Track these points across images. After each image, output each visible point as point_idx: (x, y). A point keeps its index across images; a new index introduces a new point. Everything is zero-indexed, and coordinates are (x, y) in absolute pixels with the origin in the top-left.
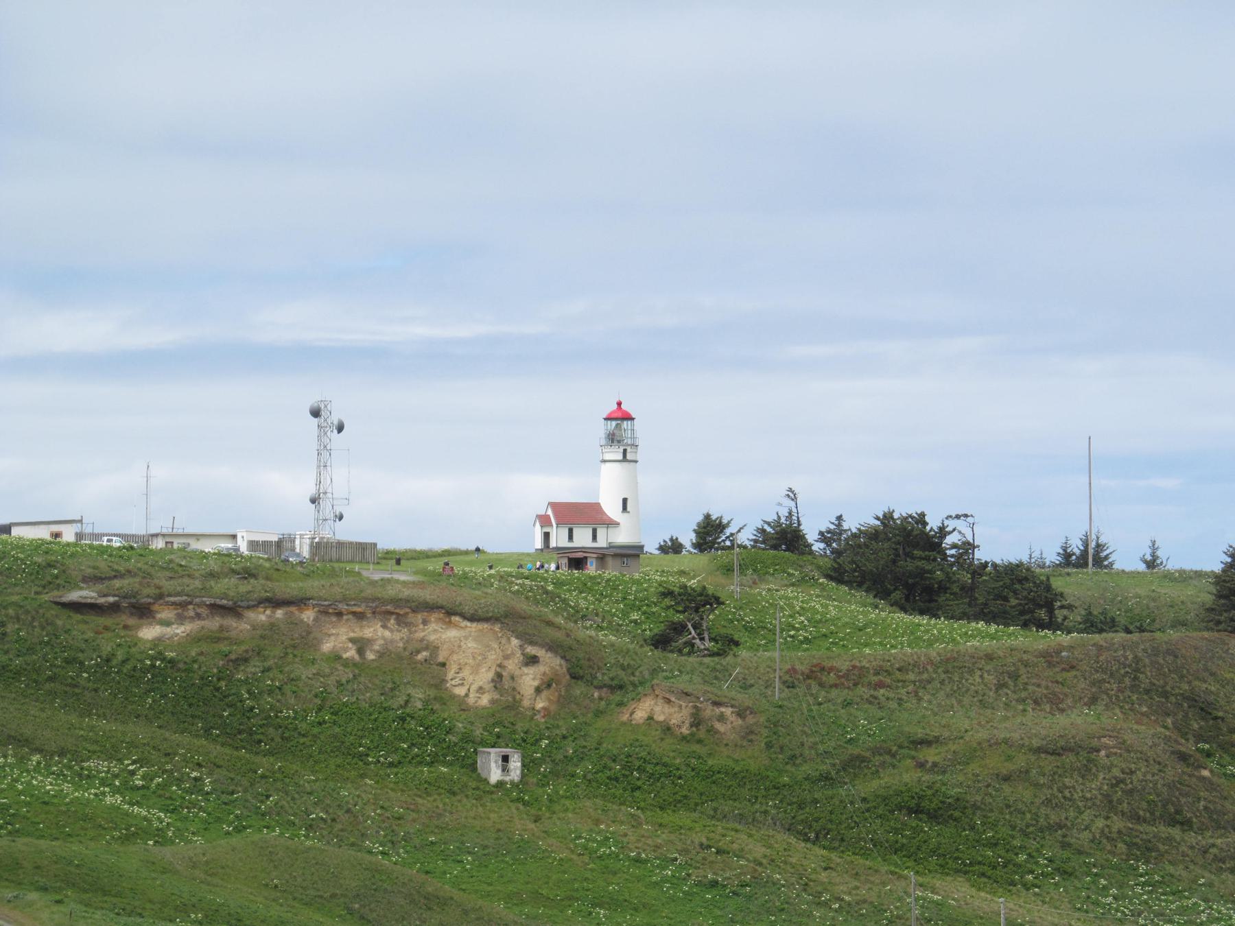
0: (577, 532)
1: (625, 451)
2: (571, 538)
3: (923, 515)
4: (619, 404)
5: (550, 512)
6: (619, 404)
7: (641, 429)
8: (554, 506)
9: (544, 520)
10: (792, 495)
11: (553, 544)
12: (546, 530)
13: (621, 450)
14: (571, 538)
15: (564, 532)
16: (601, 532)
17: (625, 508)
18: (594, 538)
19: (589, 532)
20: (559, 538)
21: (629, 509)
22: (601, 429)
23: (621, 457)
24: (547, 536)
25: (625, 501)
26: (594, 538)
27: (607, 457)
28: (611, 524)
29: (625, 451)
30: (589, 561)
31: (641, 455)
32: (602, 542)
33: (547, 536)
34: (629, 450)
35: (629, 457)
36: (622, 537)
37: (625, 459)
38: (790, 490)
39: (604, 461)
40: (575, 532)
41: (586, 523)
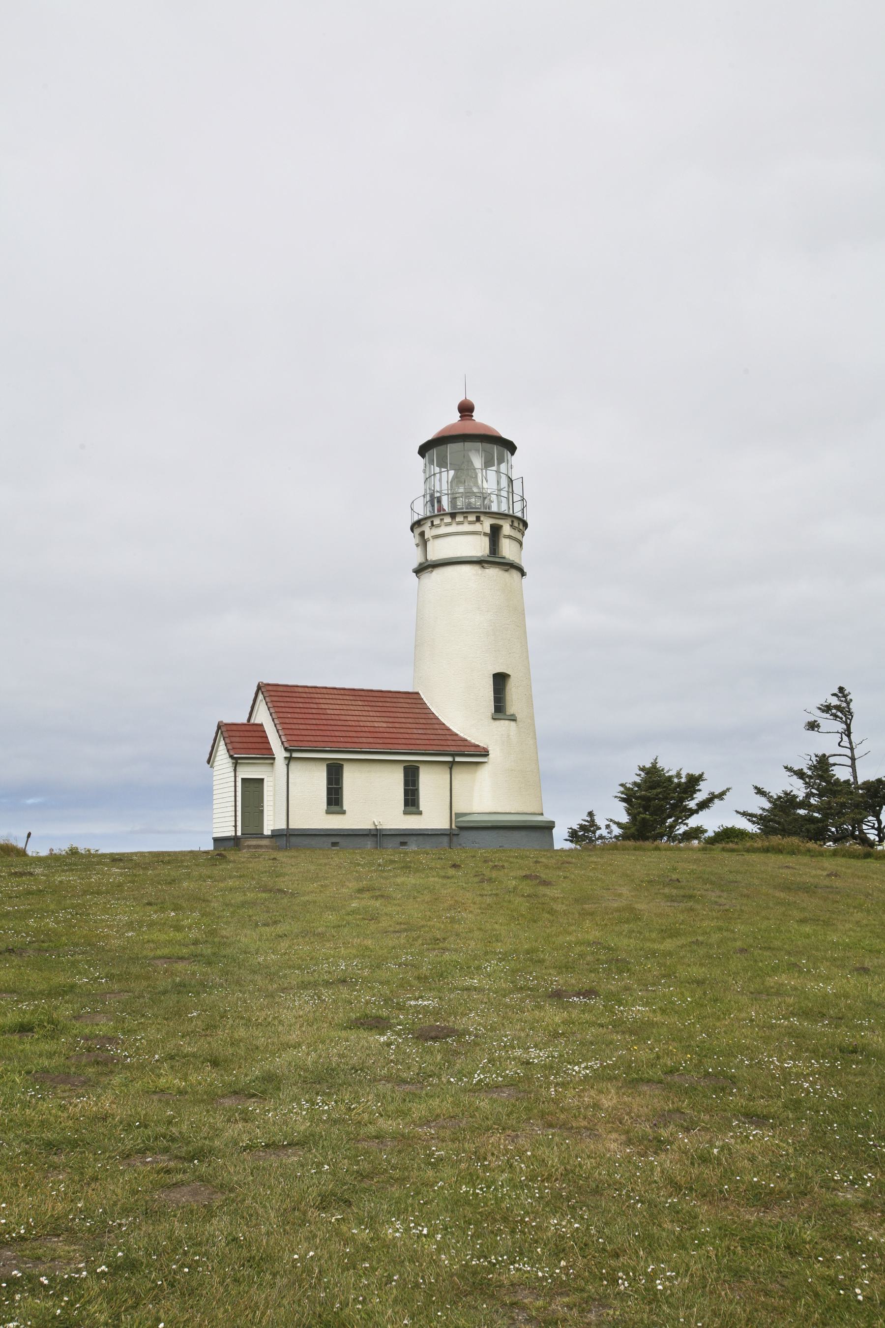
1: (495, 531)
2: (335, 799)
4: (466, 410)
6: (466, 410)
7: (534, 476)
9: (244, 742)
12: (249, 772)
13: (486, 525)
14: (335, 799)
17: (500, 708)
18: (411, 801)
19: (395, 779)
20: (296, 796)
21: (511, 709)
22: (412, 482)
23: (479, 547)
25: (500, 680)
26: (411, 801)
27: (439, 550)
28: (463, 755)
29: (495, 531)
31: (529, 550)
32: (433, 816)
33: (252, 791)
34: (507, 529)
35: (507, 549)
37: (493, 559)
38: (841, 689)
41: (375, 746)
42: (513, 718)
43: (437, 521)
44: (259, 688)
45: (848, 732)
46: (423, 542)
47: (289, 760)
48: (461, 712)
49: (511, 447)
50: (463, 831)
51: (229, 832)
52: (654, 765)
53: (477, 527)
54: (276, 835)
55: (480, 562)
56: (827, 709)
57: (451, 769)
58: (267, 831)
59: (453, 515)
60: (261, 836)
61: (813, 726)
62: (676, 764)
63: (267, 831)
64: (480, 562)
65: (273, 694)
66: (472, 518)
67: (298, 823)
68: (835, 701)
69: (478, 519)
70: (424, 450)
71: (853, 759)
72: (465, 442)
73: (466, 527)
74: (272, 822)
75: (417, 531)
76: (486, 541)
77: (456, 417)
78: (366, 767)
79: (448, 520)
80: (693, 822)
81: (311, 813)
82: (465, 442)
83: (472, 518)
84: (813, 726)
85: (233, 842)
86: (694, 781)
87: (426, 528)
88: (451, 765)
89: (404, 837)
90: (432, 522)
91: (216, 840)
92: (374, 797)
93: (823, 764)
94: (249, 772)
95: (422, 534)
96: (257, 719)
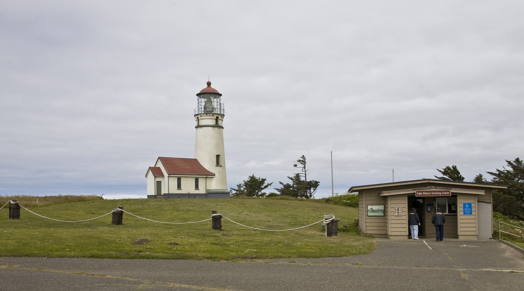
0: (183, 181)
1: (217, 118)
2: (179, 186)
3: (455, 168)
4: (209, 84)
5: (160, 165)
6: (209, 84)
8: (164, 160)
9: (156, 172)
10: (303, 161)
11: (164, 191)
12: (158, 179)
14: (179, 186)
15: (174, 182)
16: (201, 182)
17: (218, 164)
18: (197, 187)
19: (192, 182)
20: (169, 185)
21: (221, 164)
23: (213, 122)
24: (159, 185)
26: (197, 187)
27: (202, 123)
28: (208, 175)
29: (217, 118)
30: (461, 203)
31: (225, 122)
32: (202, 190)
34: (220, 118)
35: (220, 123)
36: (214, 185)
38: (303, 156)
39: (198, 126)
40: (183, 180)
42: (221, 166)
44: (159, 158)
45: (305, 168)
46: (198, 120)
47: (169, 177)
48: (208, 164)
49: (221, 95)
50: (210, 194)
51: (153, 194)
52: (253, 176)
53: (213, 117)
54: (164, 195)
55: (213, 126)
56: (299, 161)
58: (162, 194)
59: (207, 114)
60: (161, 195)
61: (295, 166)
62: (258, 176)
63: (162, 194)
64: (213, 126)
65: (165, 161)
66: (211, 115)
67: (171, 192)
68: (301, 159)
70: (198, 95)
71: (306, 175)
72: (209, 94)
73: (210, 117)
74: (164, 191)
75: (196, 117)
76: (215, 121)
77: (206, 86)
78: (186, 179)
79: (205, 115)
80: (263, 191)
81: (174, 190)
82: (209, 94)
83: (211, 115)
84: (295, 166)
85: (155, 196)
86: (263, 180)
87: (199, 116)
88: (206, 178)
89: (195, 195)
91: (148, 196)
92: (188, 186)
93: (298, 176)
94: (158, 179)
95: (198, 118)
96: (158, 166)
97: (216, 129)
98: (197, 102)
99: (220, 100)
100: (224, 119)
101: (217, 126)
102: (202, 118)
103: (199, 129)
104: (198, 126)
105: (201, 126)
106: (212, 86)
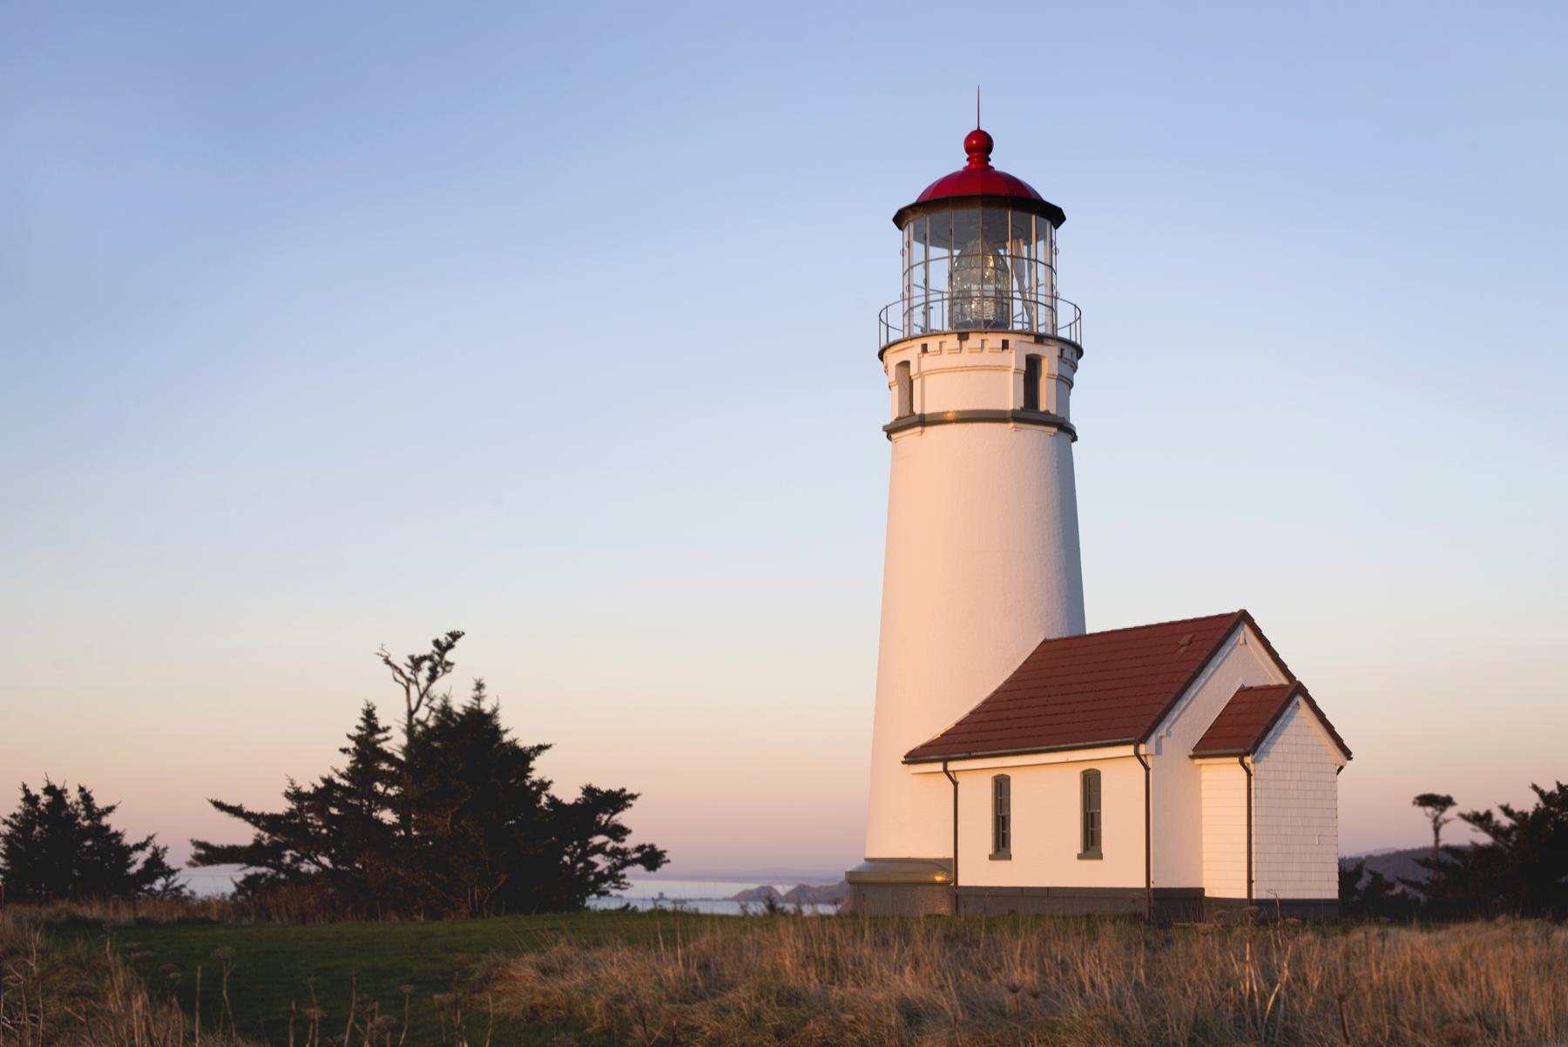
1: (1033, 364)
6: (980, 144)
37: (1029, 413)
39: (909, 421)
43: (933, 343)
46: (906, 379)
49: (1055, 216)
57: (956, 784)
59: (963, 337)
69: (1005, 345)
79: (953, 341)
90: (925, 348)
97: (1033, 437)
98: (898, 264)
99: (1052, 249)
100: (1077, 377)
101: (1040, 412)
102: (928, 362)
103: (909, 437)
104: (909, 421)
105: (924, 421)
106: (1000, 161)
